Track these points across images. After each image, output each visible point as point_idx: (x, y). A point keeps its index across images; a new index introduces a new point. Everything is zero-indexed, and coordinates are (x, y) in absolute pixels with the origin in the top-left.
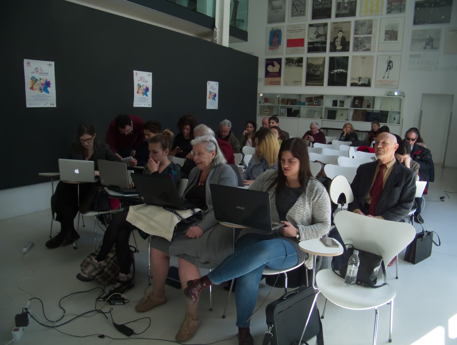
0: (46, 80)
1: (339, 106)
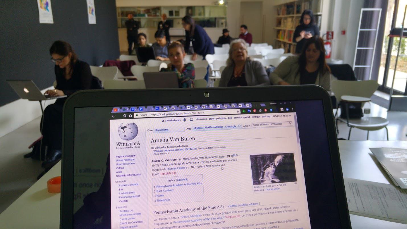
1: (176, 15)
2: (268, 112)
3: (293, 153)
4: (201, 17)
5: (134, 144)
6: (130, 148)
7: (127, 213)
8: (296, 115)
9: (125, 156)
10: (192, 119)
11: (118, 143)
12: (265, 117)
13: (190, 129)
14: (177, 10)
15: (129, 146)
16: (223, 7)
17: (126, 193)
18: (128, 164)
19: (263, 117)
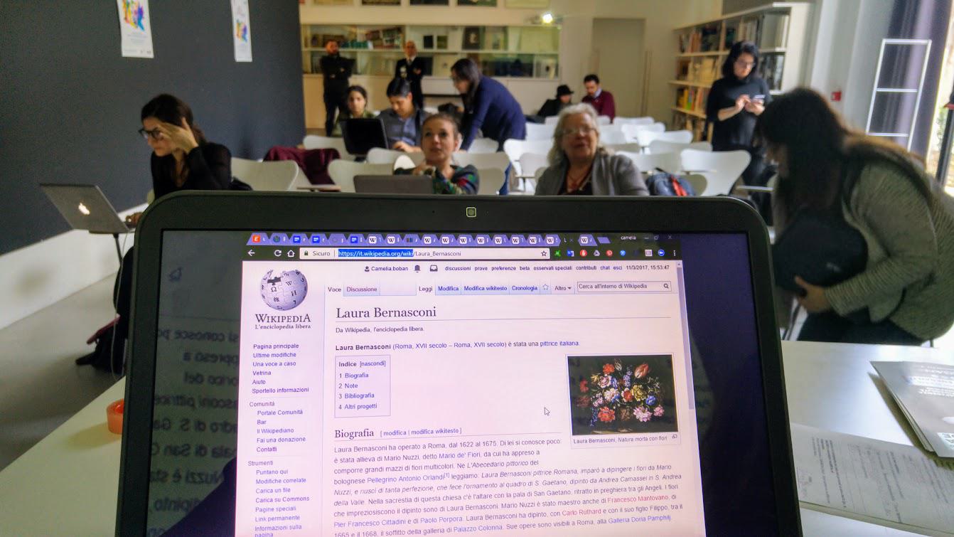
0: (139, 4)
1: (439, 47)
2: (616, 257)
3: (670, 356)
4: (498, 53)
5: (296, 319)
6: (288, 327)
7: (273, 477)
8: (681, 266)
9: (275, 347)
10: (434, 268)
11: (259, 316)
12: (608, 268)
13: (429, 290)
14: (442, 33)
15: (285, 323)
16: (552, 31)
17: (273, 432)
18: (281, 364)
19: (603, 268)
